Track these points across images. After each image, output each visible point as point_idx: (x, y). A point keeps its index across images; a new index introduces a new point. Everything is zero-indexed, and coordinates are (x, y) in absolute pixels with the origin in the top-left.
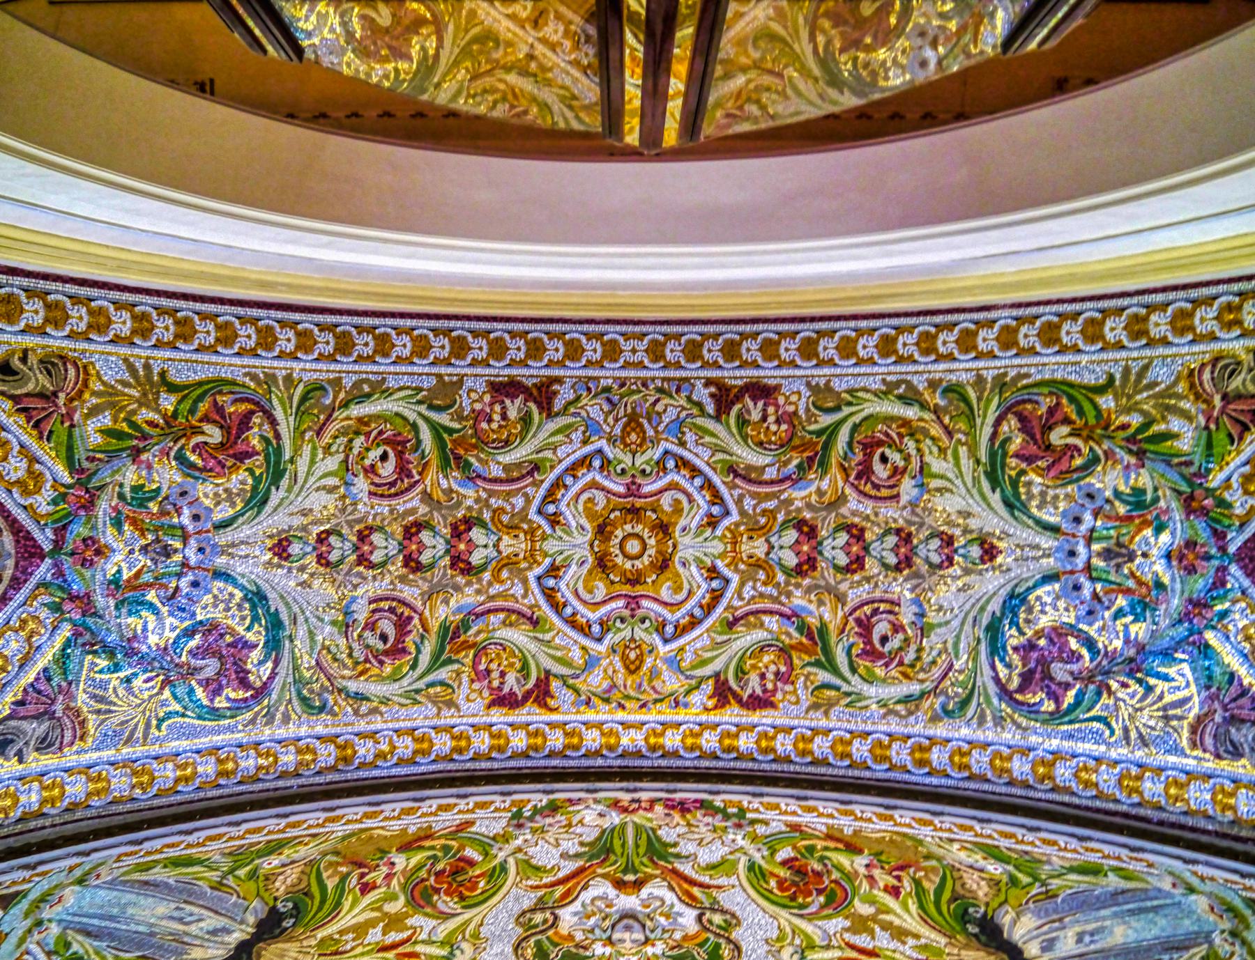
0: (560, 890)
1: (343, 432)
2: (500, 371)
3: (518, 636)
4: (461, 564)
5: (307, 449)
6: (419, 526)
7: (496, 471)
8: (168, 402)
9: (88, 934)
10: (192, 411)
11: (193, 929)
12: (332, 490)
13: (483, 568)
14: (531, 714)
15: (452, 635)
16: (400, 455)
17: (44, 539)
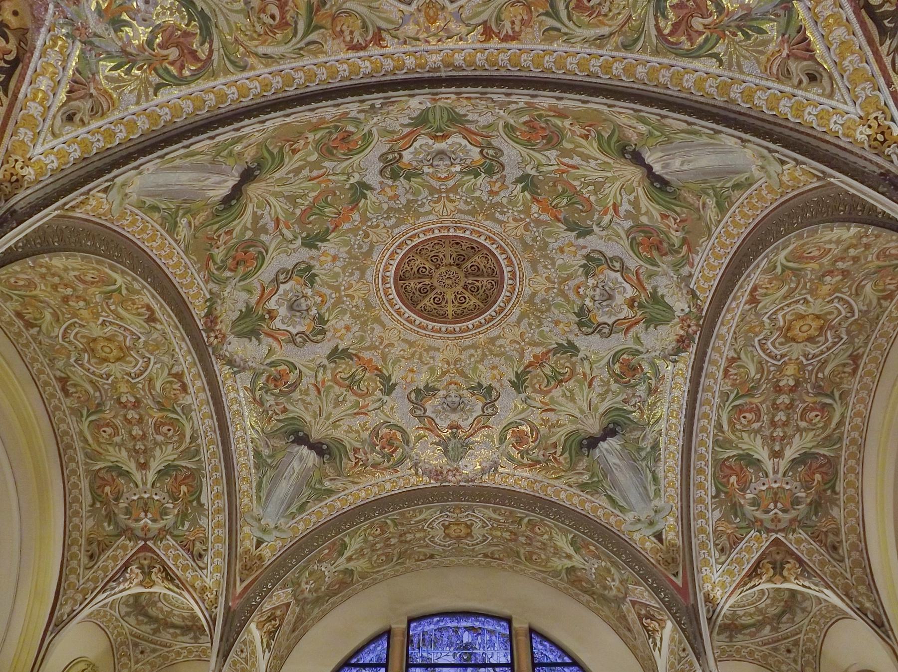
0: (280, 337)
1: (99, 446)
2: (60, 394)
3: (158, 385)
4: (137, 404)
5: (108, 458)
6: (126, 419)
7: (97, 394)
8: (98, 505)
9: (289, 507)
10: (100, 496)
11: (297, 470)
12: (120, 450)
13: (136, 397)
14: (187, 379)
15: (162, 408)
16: (102, 426)
17: (141, 543)
